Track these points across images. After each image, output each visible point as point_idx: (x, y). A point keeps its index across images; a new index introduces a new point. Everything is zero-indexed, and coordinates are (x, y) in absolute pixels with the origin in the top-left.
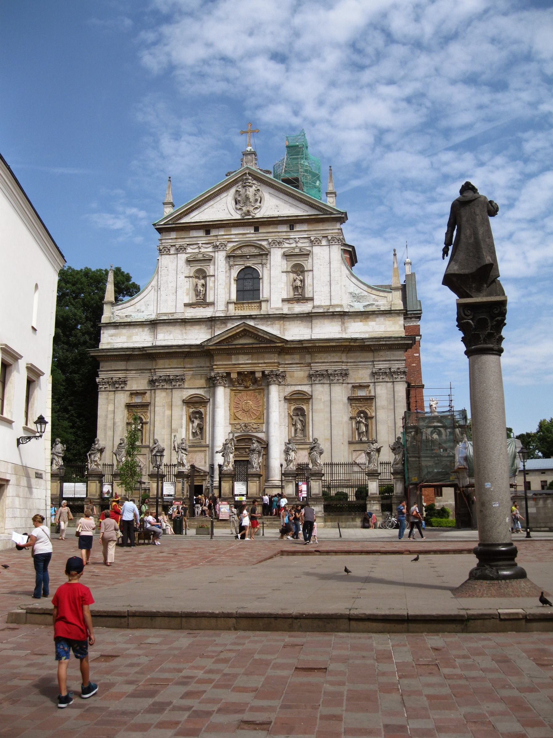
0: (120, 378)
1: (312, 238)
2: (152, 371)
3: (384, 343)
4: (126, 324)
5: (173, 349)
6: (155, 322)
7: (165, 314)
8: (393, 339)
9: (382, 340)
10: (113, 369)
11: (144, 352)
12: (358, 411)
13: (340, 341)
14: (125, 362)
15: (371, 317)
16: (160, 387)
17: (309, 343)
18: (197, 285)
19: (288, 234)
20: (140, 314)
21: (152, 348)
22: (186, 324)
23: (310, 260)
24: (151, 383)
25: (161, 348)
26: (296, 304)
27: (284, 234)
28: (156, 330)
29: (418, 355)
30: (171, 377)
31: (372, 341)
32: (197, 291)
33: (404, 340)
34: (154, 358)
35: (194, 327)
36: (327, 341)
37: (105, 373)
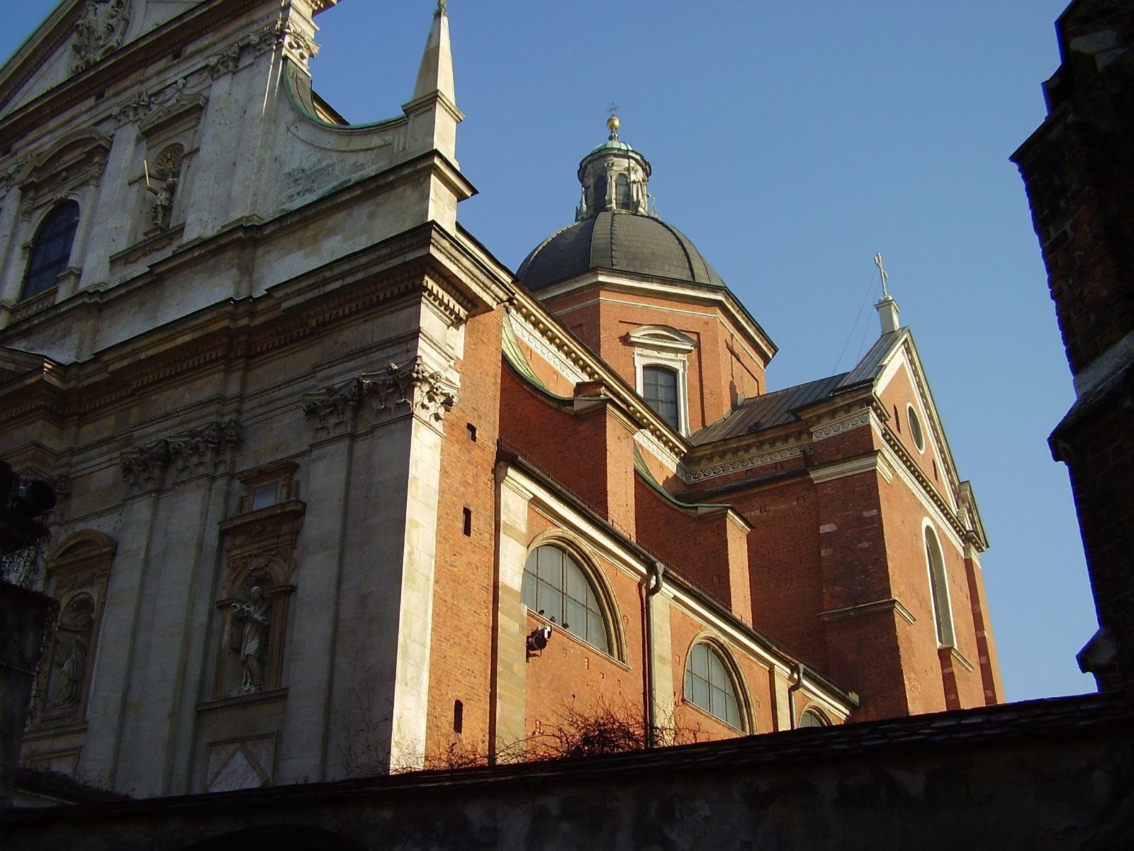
1: (213, 61)
3: (337, 285)
8: (363, 260)
9: (328, 274)
12: (243, 576)
13: (200, 321)
15: (331, 222)
17: (123, 358)
19: (162, 77)
23: (200, 127)
26: (140, 260)
27: (155, 81)
29: (874, 512)
31: (300, 292)
33: (401, 251)
36: (166, 334)
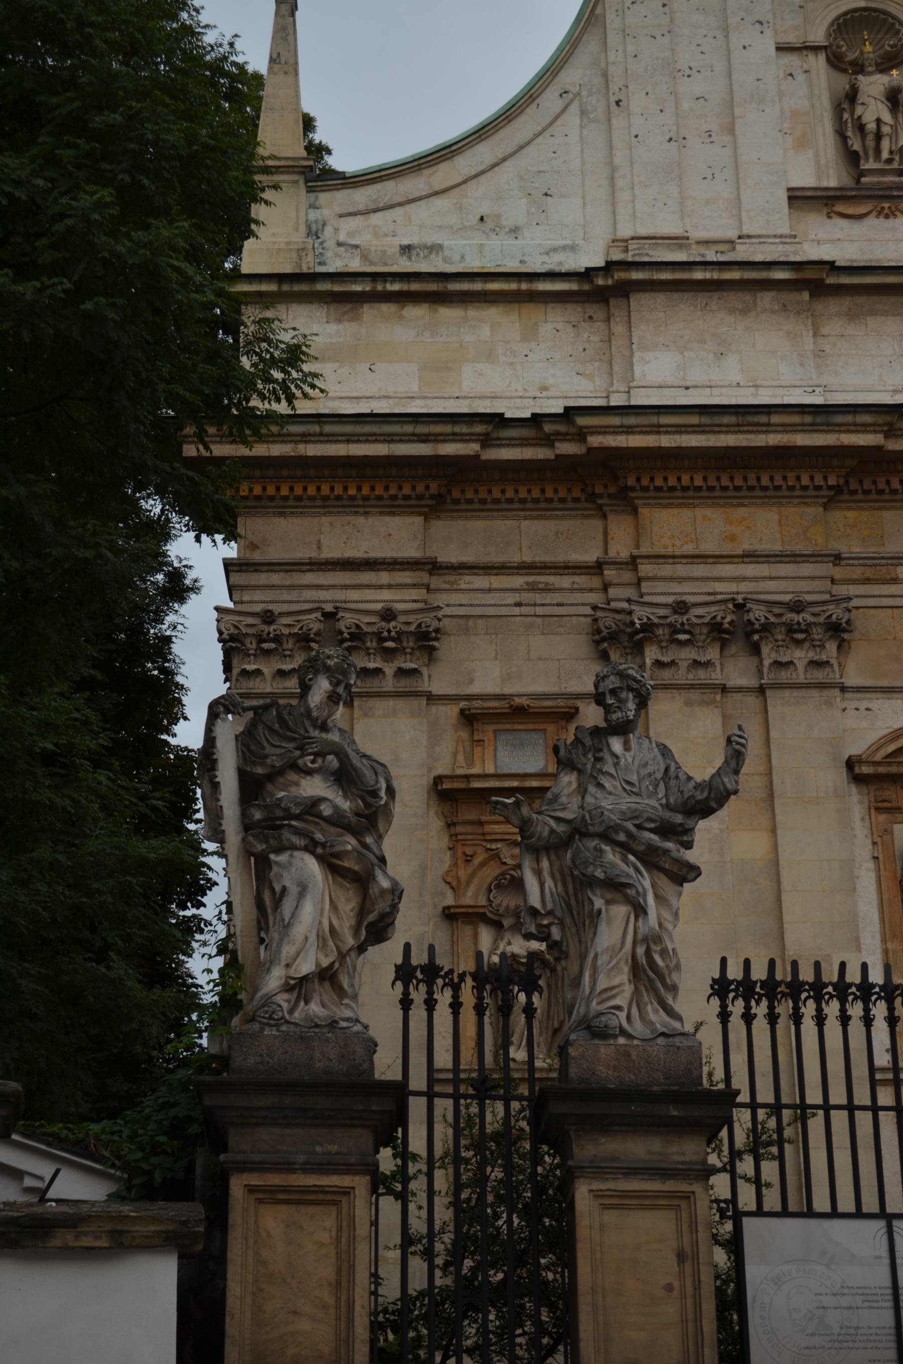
0: (388, 615)
2: (609, 573)
4: (415, 286)
5: (768, 428)
6: (620, 275)
7: (678, 241)
10: (331, 552)
11: (567, 448)
14: (419, 520)
16: (682, 675)
18: (852, 96)
20: (495, 243)
21: (632, 420)
22: (819, 307)
24: (604, 656)
25: (694, 420)
28: (619, 328)
30: (758, 613)
32: (861, 128)
34: (627, 489)
35: (872, 322)
37: (276, 579)
